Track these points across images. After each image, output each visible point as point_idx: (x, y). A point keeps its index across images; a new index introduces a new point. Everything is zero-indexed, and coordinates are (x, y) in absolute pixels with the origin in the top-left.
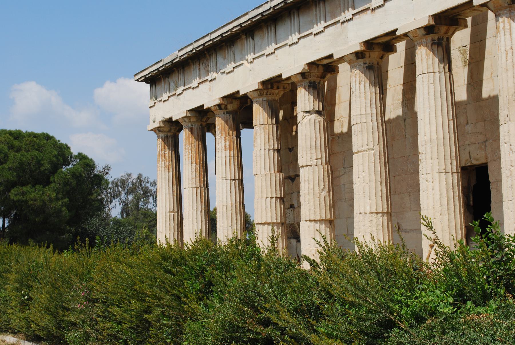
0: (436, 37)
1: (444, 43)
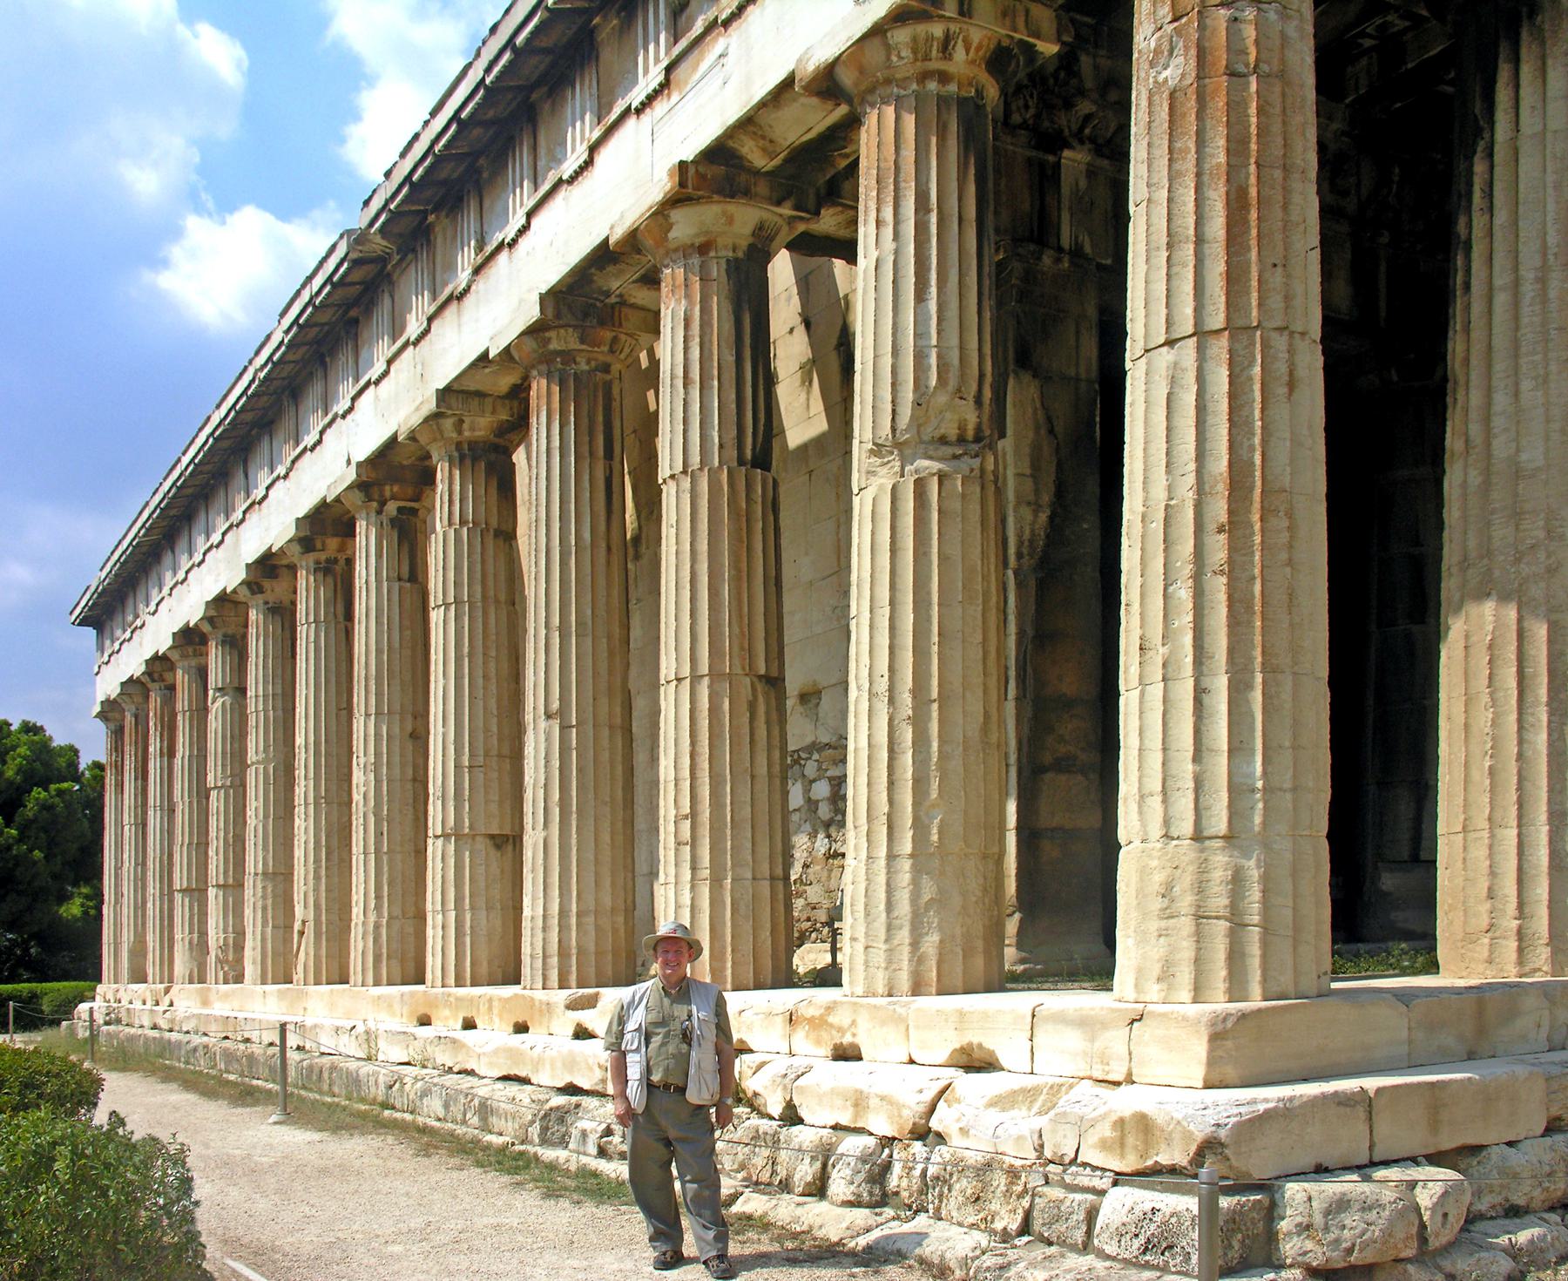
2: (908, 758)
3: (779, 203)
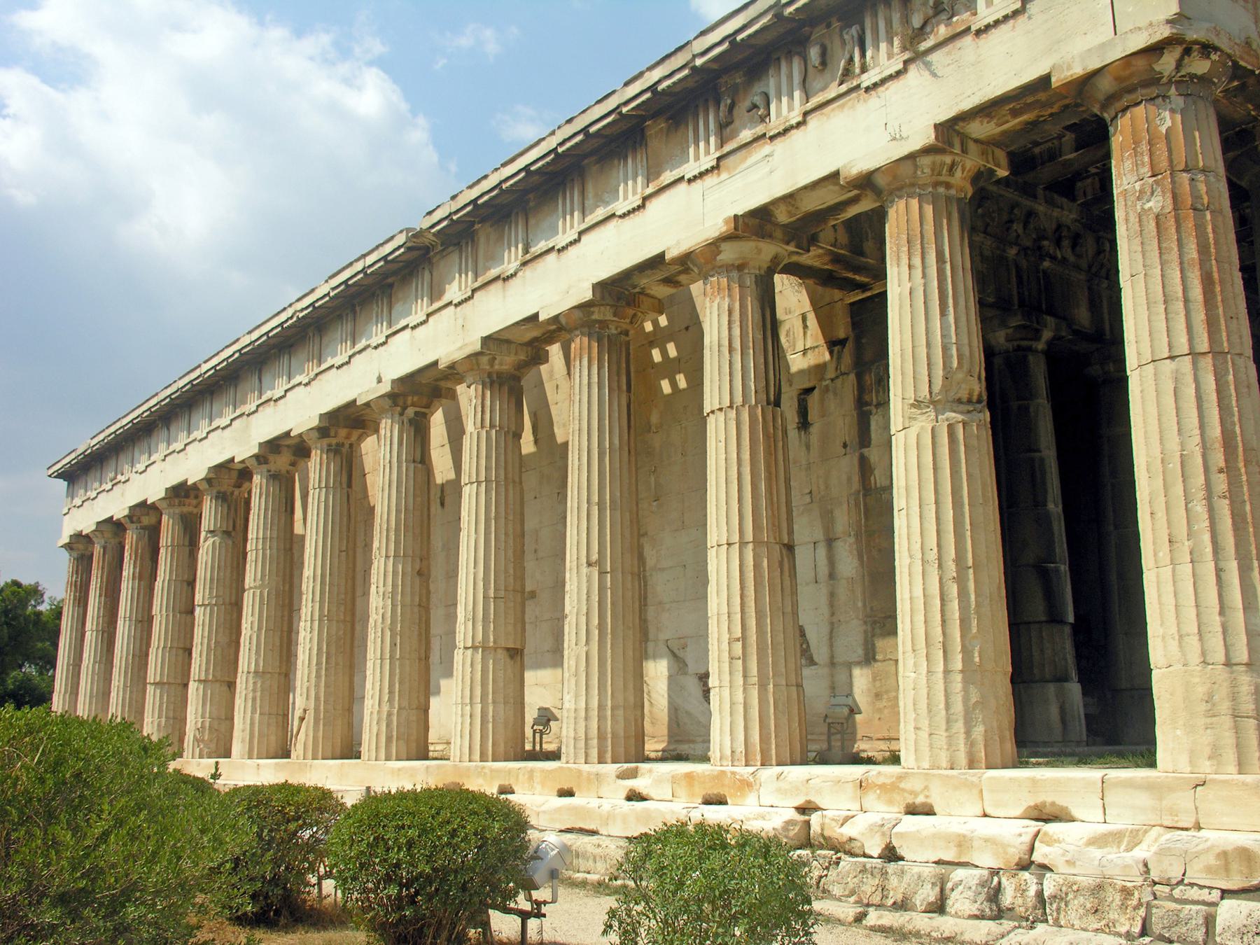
0: (334, 441)
1: (345, 450)
2: (955, 605)
3: (788, 243)
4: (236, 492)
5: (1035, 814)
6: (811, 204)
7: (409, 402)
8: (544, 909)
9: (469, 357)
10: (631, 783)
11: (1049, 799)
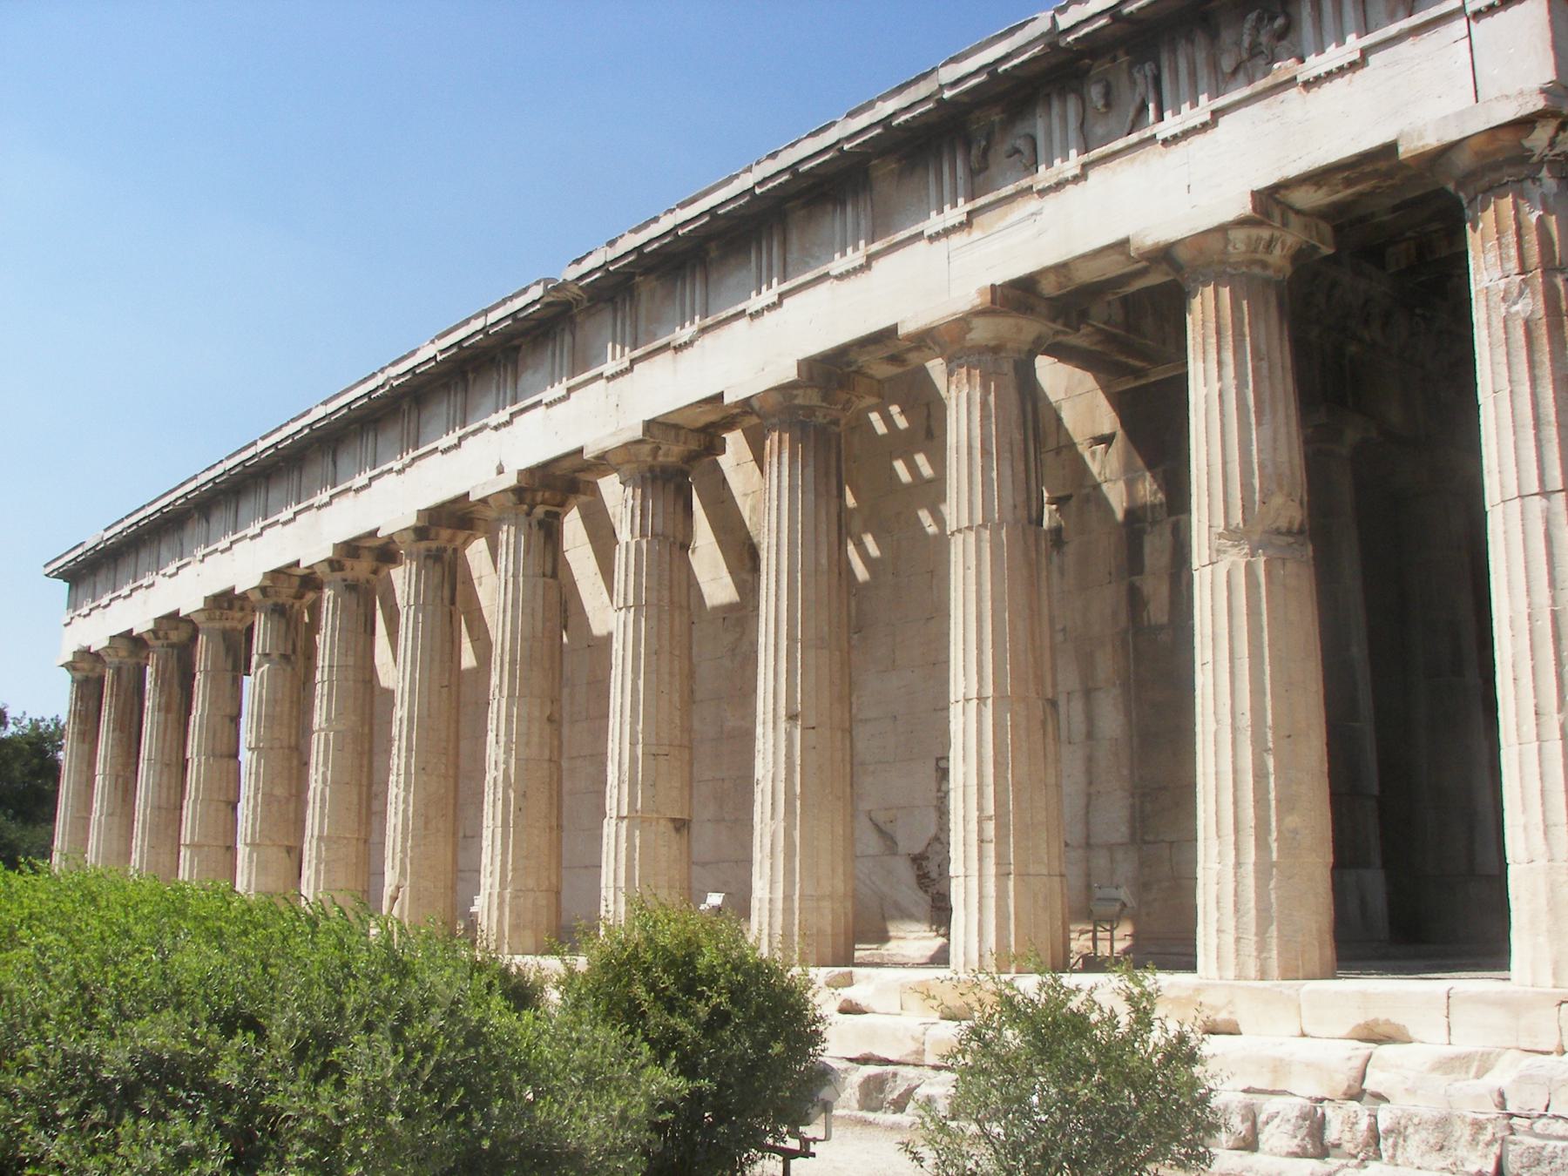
0: (434, 545)
3: (1054, 320)
4: (297, 606)
5: (1365, 1034)
6: (1085, 275)
7: (539, 497)
8: (813, 1148)
9: (626, 445)
10: (847, 993)
11: (1382, 1017)
